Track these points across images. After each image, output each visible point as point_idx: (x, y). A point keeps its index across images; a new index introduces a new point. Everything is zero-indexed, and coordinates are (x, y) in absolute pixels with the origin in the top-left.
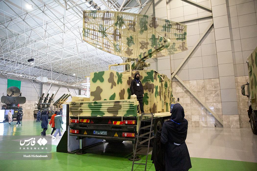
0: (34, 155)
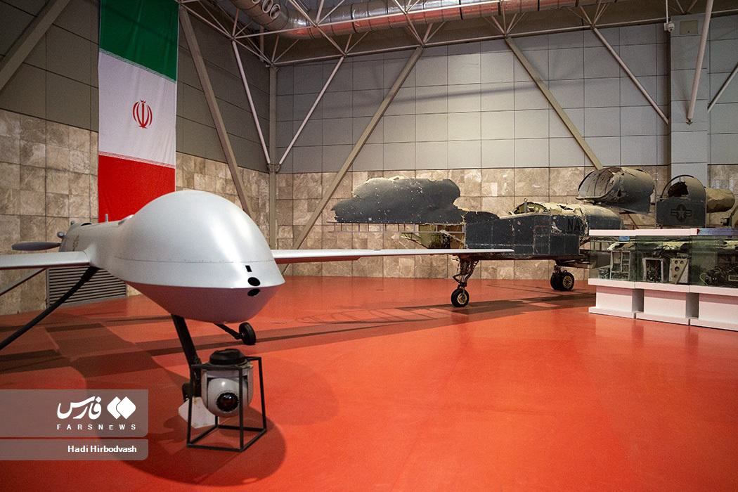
0: (97, 447)
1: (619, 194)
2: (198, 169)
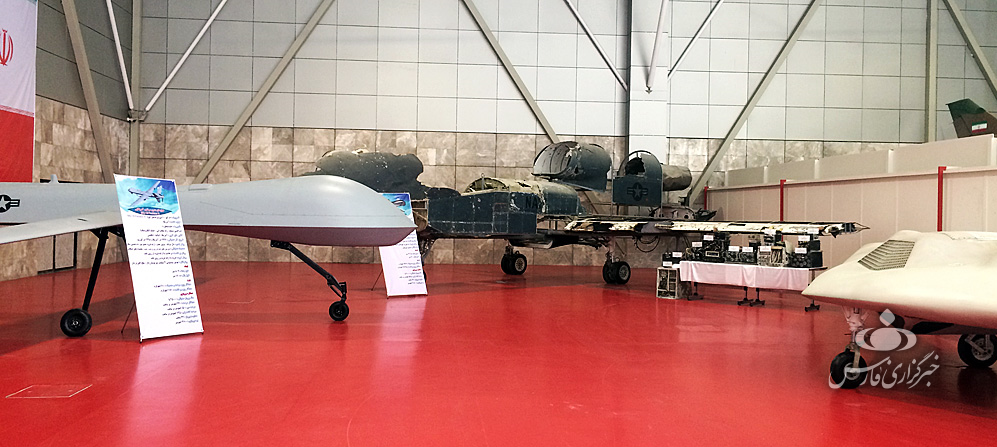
1: (576, 171)
2: (56, 117)
